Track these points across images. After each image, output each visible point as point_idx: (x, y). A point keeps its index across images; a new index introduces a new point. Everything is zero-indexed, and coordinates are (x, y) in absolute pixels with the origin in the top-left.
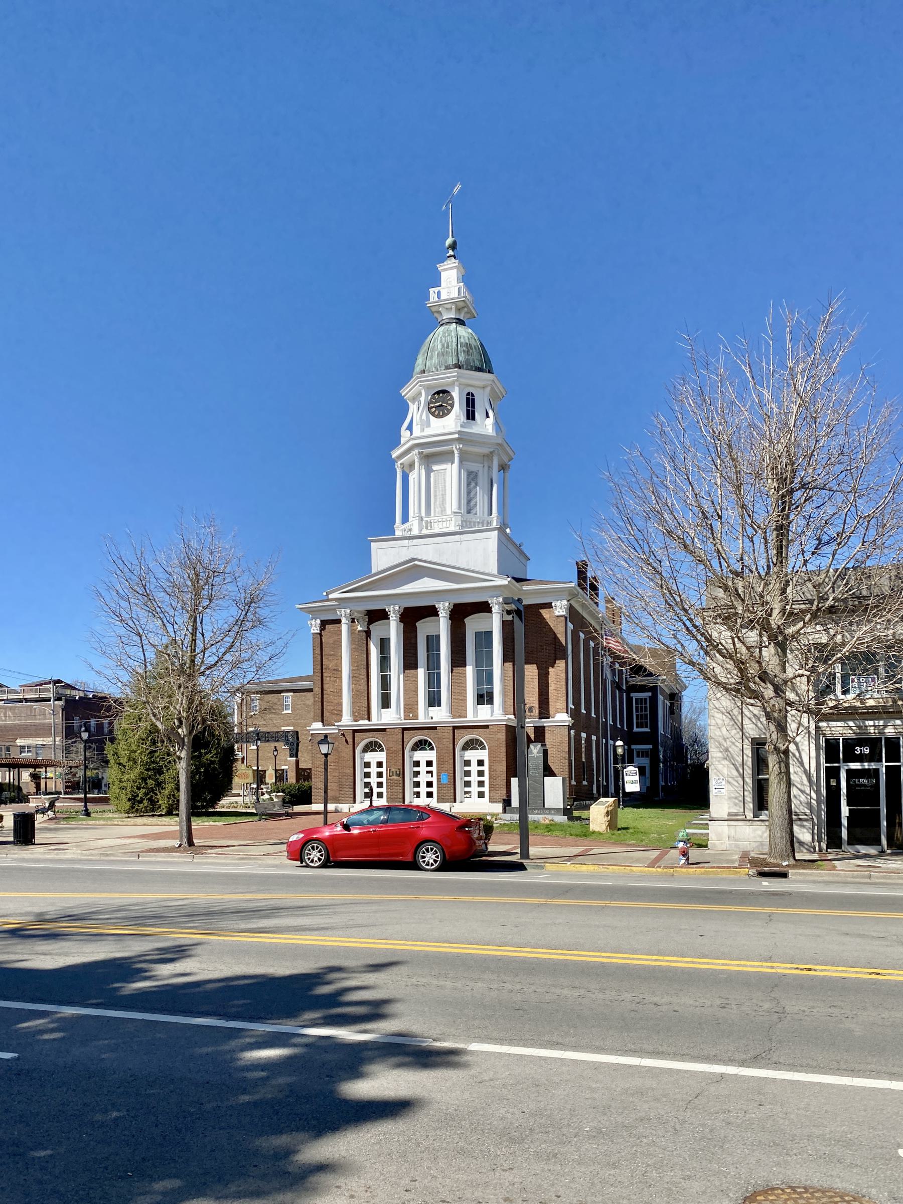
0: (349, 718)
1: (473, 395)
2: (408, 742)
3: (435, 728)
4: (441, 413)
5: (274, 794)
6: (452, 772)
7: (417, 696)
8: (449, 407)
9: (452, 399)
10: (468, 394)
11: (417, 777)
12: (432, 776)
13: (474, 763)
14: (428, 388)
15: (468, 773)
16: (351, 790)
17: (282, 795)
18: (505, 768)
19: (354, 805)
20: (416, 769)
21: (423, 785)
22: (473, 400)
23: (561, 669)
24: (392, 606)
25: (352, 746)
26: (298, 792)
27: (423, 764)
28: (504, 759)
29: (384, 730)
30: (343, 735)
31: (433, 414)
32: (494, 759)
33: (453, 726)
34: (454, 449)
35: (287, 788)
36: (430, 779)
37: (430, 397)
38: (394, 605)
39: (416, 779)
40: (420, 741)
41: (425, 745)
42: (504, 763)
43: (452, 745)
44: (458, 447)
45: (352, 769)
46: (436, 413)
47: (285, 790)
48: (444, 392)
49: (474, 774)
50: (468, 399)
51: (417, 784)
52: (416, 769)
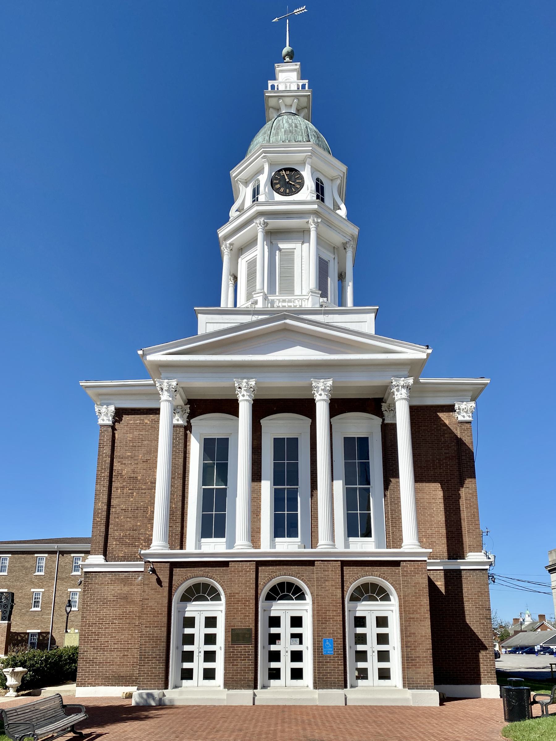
0: (163, 543)
1: (322, 183)
2: (265, 584)
3: (311, 563)
4: (288, 190)
5: (10, 669)
6: (340, 636)
7: (260, 519)
8: (298, 186)
9: (302, 178)
10: (318, 179)
11: (275, 643)
12: (301, 643)
13: (371, 622)
14: (271, 165)
15: (361, 639)
16: (162, 666)
17: (21, 672)
18: (429, 631)
19: (165, 691)
20: (274, 630)
21: (285, 657)
22: (322, 188)
23: (471, 492)
24: (245, 380)
25: (166, 589)
26: (46, 666)
27: (285, 622)
28: (428, 615)
29: (225, 564)
30: (153, 571)
31: (278, 191)
32: (411, 616)
33: (342, 562)
34: (311, 221)
35: (30, 659)
36: (297, 648)
37: (273, 173)
38: (249, 378)
39: (273, 648)
40: (281, 585)
41: (289, 591)
42: (428, 623)
43: (339, 591)
44: (316, 220)
45: (165, 629)
46: (282, 190)
47: (25, 661)
48: (291, 170)
49: (372, 639)
50: (317, 185)
51: (275, 656)
52: (274, 630)
